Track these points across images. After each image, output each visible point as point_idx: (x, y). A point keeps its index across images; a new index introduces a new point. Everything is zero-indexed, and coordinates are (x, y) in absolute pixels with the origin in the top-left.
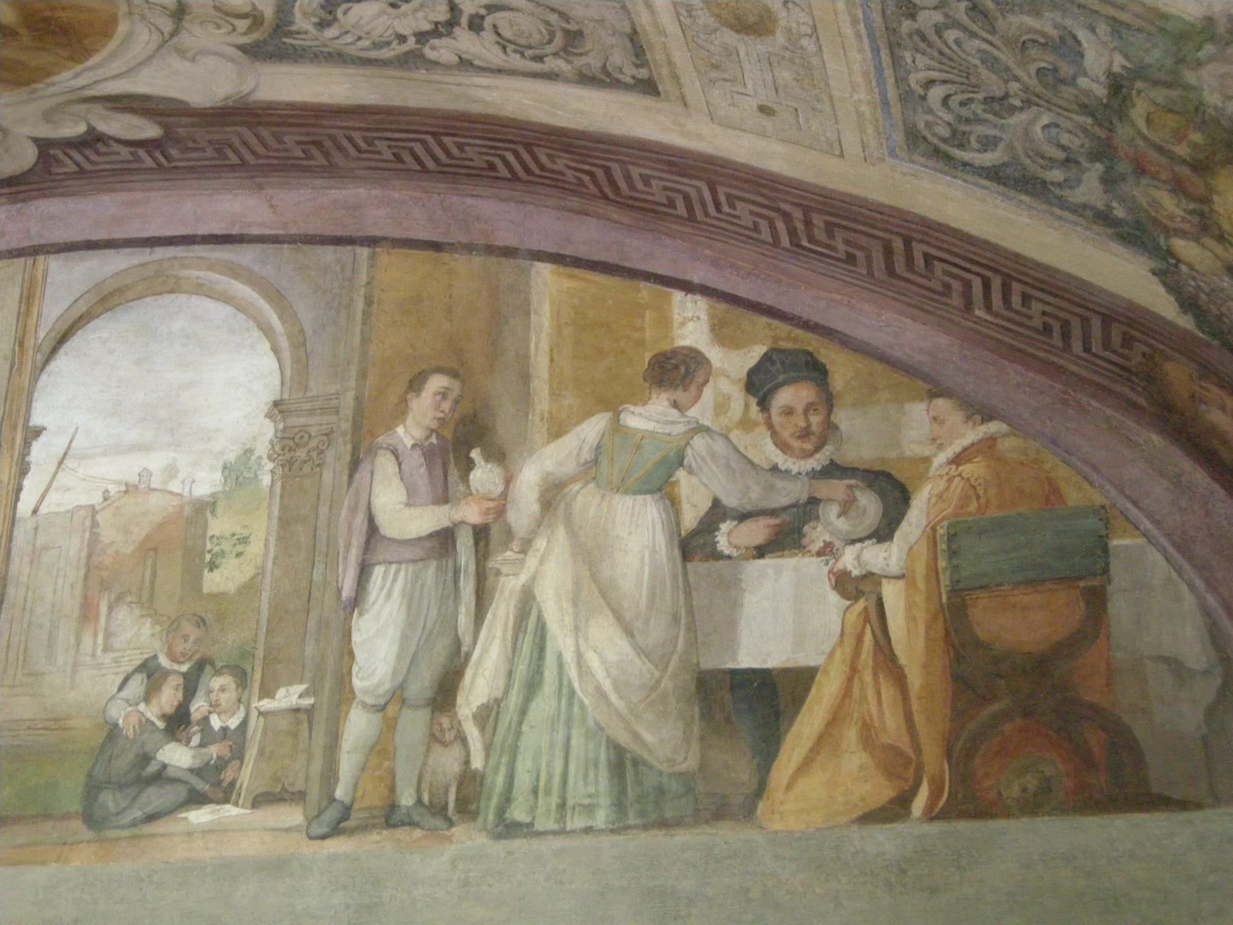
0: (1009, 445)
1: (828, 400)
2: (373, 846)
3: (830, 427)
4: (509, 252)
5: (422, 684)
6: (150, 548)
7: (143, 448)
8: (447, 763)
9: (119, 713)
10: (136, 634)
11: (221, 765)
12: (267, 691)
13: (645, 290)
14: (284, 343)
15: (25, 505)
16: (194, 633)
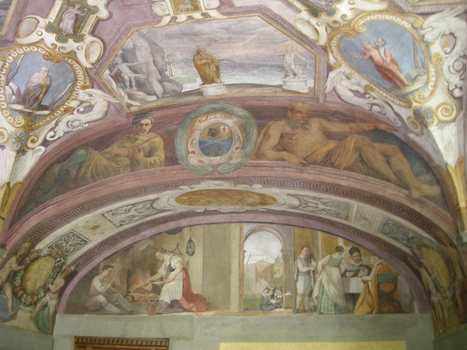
0: (385, 263)
1: (360, 255)
2: (303, 315)
3: (361, 260)
4: (314, 229)
5: (308, 292)
6: (265, 270)
7: (262, 255)
8: (312, 304)
9: (264, 295)
10: (265, 284)
11: (280, 303)
12: (285, 293)
13: (334, 237)
14: (282, 240)
15: (245, 263)
16: (274, 284)
